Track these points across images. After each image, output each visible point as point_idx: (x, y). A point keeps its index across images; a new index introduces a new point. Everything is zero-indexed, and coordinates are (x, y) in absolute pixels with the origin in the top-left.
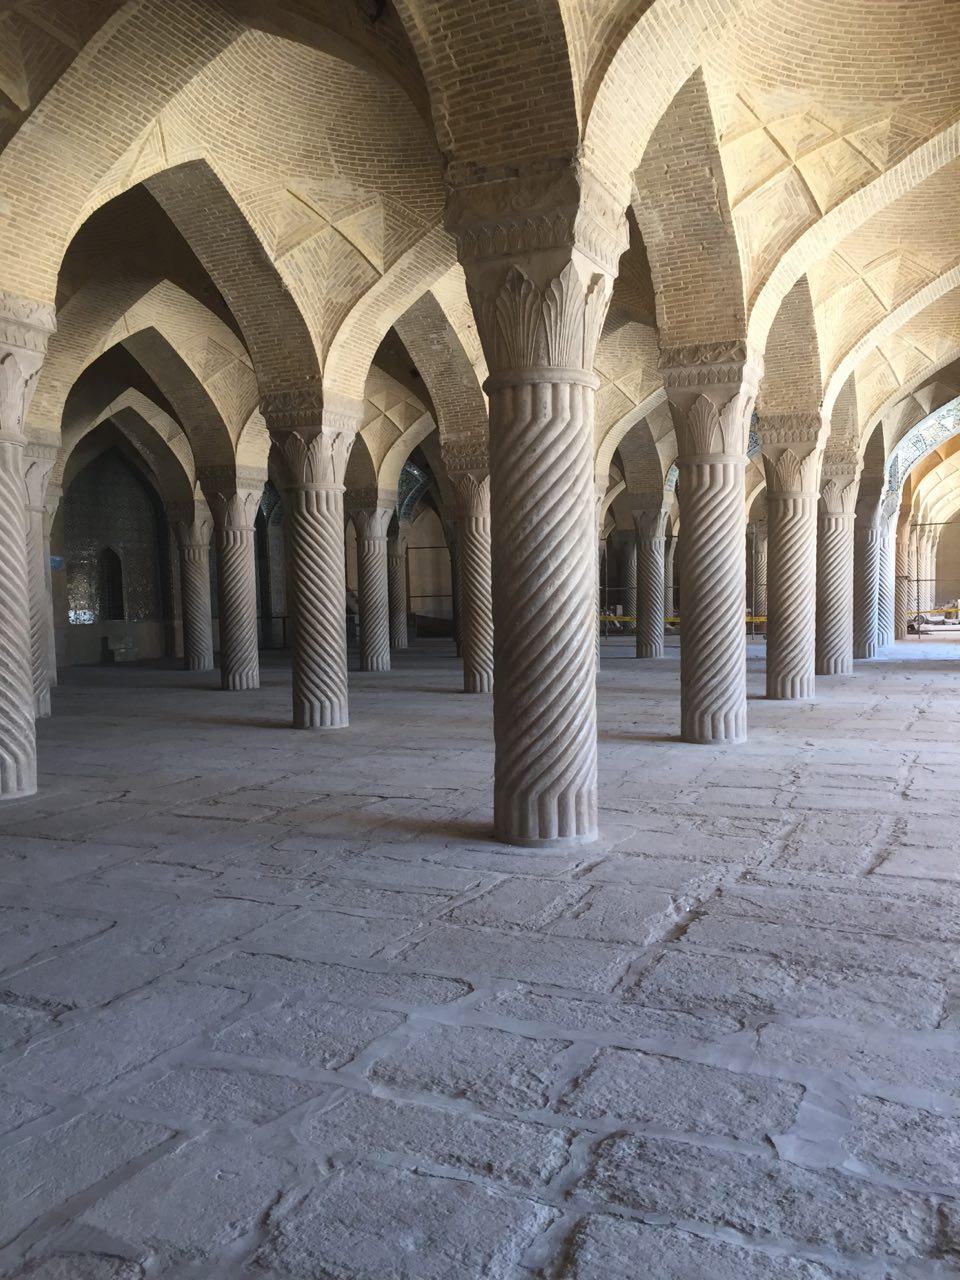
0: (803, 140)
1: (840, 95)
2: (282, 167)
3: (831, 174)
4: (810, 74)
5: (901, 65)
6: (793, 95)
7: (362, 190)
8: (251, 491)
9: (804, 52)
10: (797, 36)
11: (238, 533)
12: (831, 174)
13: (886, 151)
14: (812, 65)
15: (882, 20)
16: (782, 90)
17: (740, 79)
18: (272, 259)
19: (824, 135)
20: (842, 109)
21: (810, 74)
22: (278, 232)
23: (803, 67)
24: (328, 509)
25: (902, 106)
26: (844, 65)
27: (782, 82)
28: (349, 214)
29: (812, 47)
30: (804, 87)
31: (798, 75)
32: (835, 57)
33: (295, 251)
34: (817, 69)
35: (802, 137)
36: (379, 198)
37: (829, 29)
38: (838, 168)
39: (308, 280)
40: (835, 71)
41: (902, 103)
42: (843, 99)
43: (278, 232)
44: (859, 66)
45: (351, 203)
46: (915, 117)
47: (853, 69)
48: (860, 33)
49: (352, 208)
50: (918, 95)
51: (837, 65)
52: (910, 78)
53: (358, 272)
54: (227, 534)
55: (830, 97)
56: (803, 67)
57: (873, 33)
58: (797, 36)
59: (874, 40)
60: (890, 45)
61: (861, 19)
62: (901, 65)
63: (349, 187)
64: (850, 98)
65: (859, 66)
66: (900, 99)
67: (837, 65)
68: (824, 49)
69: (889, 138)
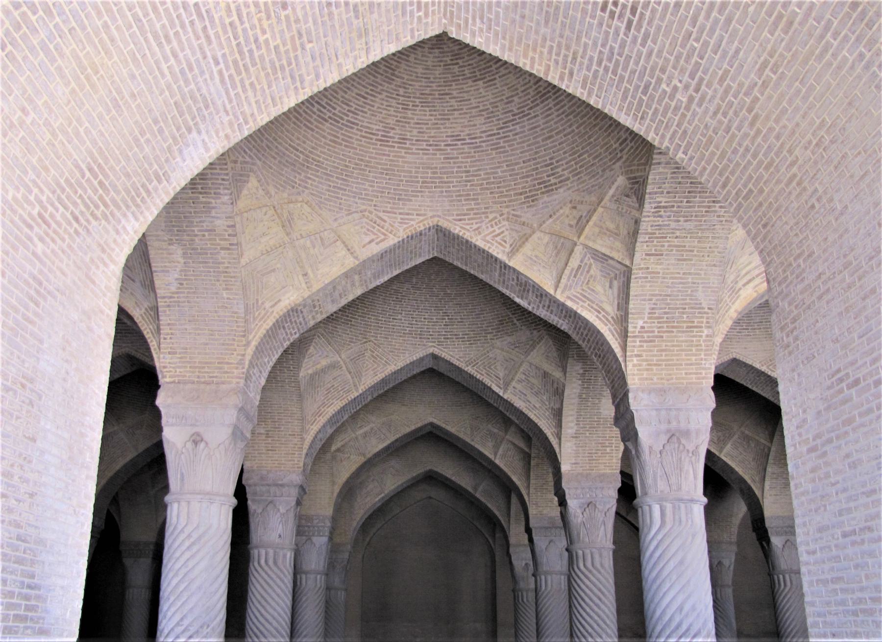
0: (577, 223)
1: (586, 178)
2: (489, 336)
3: (616, 234)
4: (561, 176)
5: (610, 134)
6: (555, 197)
7: (535, 332)
8: (788, 537)
9: (547, 166)
10: (535, 159)
11: (781, 576)
12: (616, 234)
13: (635, 200)
14: (559, 170)
15: (578, 114)
16: (546, 198)
17: (505, 211)
18: (501, 394)
19: (589, 212)
20: (592, 186)
21: (561, 176)
22: (501, 375)
23: (553, 174)
24: (584, 565)
25: (624, 162)
26: (579, 156)
27: (543, 193)
28: (532, 350)
29: (551, 159)
30: (560, 187)
31: (553, 181)
32: (570, 155)
33: (514, 384)
34: (563, 170)
35: (575, 221)
36: (545, 332)
37: (553, 142)
38: (618, 227)
39: (534, 400)
40: (576, 164)
41: (624, 159)
42: (590, 179)
43: (501, 375)
44: (587, 151)
45: (531, 342)
46: (634, 165)
47: (586, 156)
48: (573, 131)
49: (533, 347)
50: (629, 147)
51: (574, 159)
52: (619, 139)
53: (555, 385)
54: (778, 578)
55: (581, 183)
56: (553, 174)
57: (581, 125)
58: (535, 159)
59: (585, 128)
60: (595, 126)
61: (567, 122)
62: (610, 134)
63: (528, 333)
64: (594, 176)
65: (587, 151)
66: (621, 157)
67: (574, 159)
68: (560, 155)
69: (632, 189)
